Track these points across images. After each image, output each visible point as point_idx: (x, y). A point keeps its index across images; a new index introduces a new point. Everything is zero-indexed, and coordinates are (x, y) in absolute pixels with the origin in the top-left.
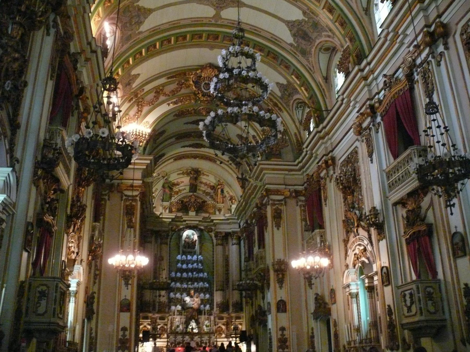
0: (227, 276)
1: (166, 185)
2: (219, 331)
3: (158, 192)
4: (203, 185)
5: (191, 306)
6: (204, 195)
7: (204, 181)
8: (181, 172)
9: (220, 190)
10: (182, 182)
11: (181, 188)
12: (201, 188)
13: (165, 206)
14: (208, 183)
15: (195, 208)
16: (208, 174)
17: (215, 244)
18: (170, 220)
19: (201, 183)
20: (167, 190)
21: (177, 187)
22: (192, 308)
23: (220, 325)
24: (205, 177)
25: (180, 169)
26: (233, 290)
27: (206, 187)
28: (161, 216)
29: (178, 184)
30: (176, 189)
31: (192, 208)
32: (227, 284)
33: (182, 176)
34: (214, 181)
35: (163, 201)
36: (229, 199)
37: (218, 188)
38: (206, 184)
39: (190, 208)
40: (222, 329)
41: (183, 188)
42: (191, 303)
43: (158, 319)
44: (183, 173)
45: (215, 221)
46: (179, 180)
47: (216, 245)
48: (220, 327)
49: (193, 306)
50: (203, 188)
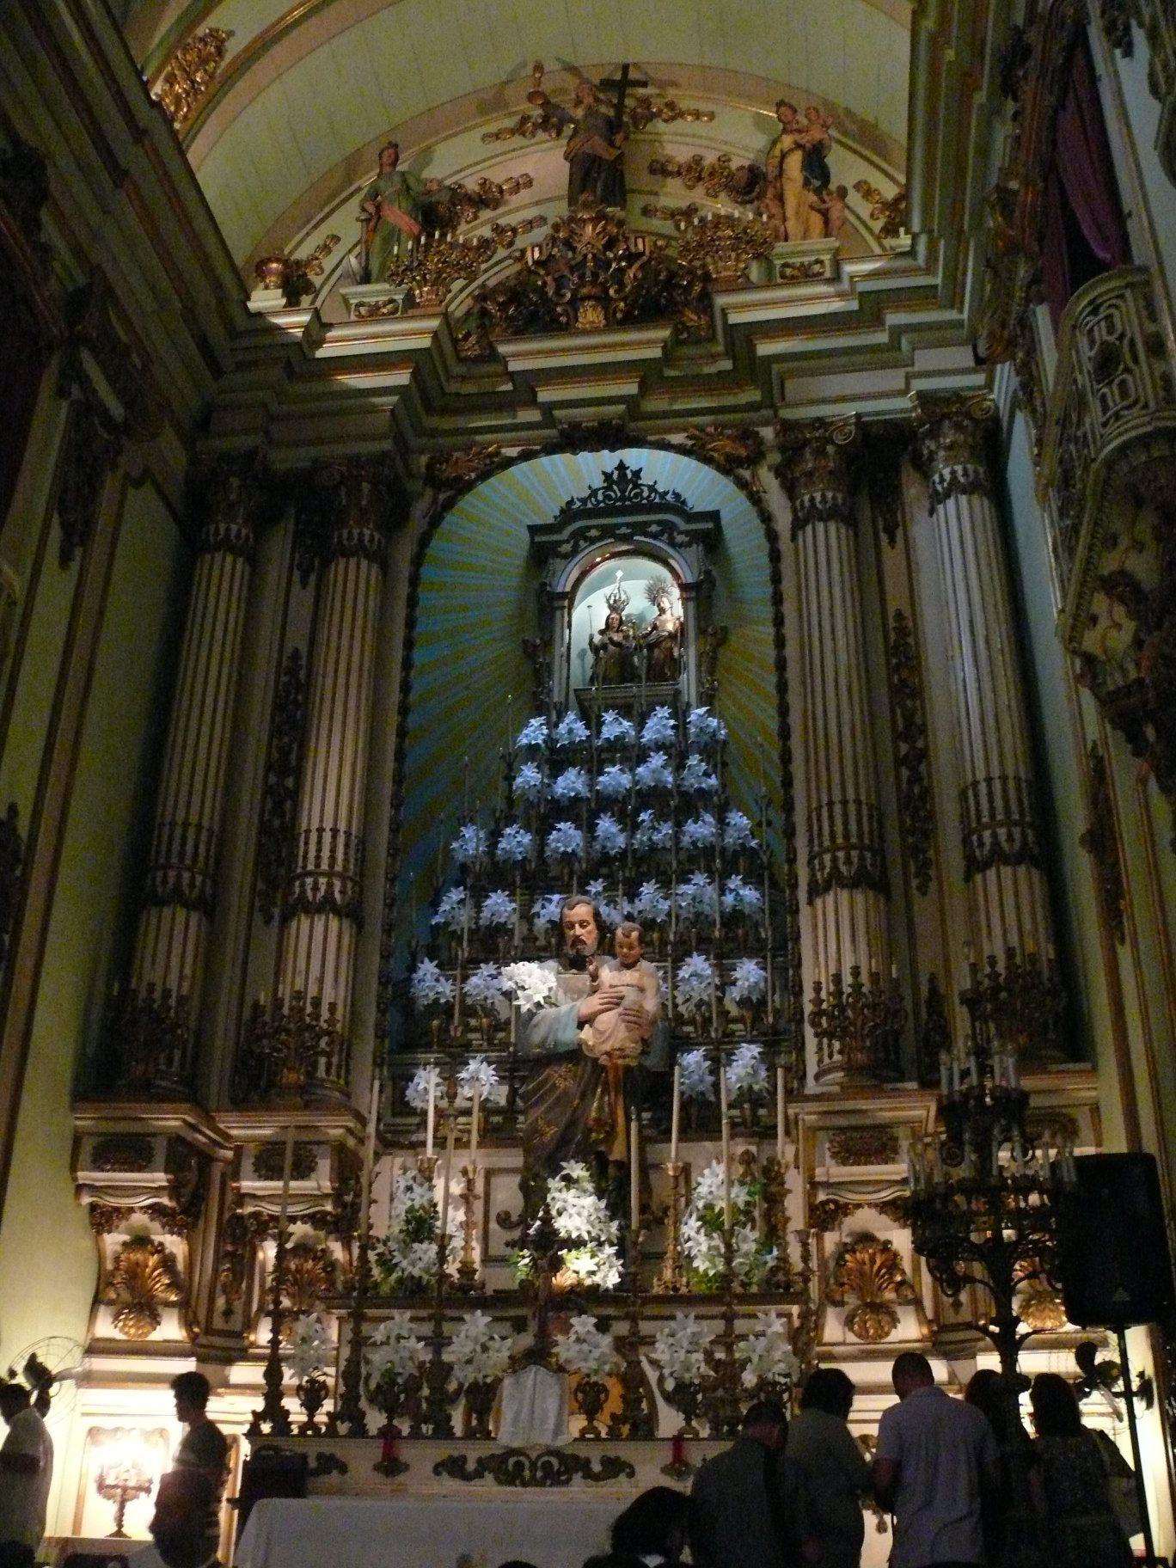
0: (916, 778)
2: (864, 1284)
3: (338, 251)
4: (674, 185)
5: (569, 1035)
8: (510, 123)
9: (795, 162)
15: (603, 300)
16: (703, 107)
17: (783, 521)
18: (402, 378)
19: (661, 169)
20: (398, 216)
21: (486, 214)
22: (575, 1055)
23: (866, 1219)
24: (686, 125)
25: (492, 103)
26: (974, 866)
27: (700, 190)
29: (487, 198)
30: (474, 229)
31: (590, 315)
32: (915, 851)
34: (759, 141)
36: (877, 226)
37: (784, 156)
38: (694, 172)
39: (575, 302)
42: (569, 1008)
43: (247, 1165)
44: (519, 129)
45: (765, 348)
46: (498, 176)
47: (798, 525)
48: (866, 1238)
49: (587, 1034)
50: (674, 195)
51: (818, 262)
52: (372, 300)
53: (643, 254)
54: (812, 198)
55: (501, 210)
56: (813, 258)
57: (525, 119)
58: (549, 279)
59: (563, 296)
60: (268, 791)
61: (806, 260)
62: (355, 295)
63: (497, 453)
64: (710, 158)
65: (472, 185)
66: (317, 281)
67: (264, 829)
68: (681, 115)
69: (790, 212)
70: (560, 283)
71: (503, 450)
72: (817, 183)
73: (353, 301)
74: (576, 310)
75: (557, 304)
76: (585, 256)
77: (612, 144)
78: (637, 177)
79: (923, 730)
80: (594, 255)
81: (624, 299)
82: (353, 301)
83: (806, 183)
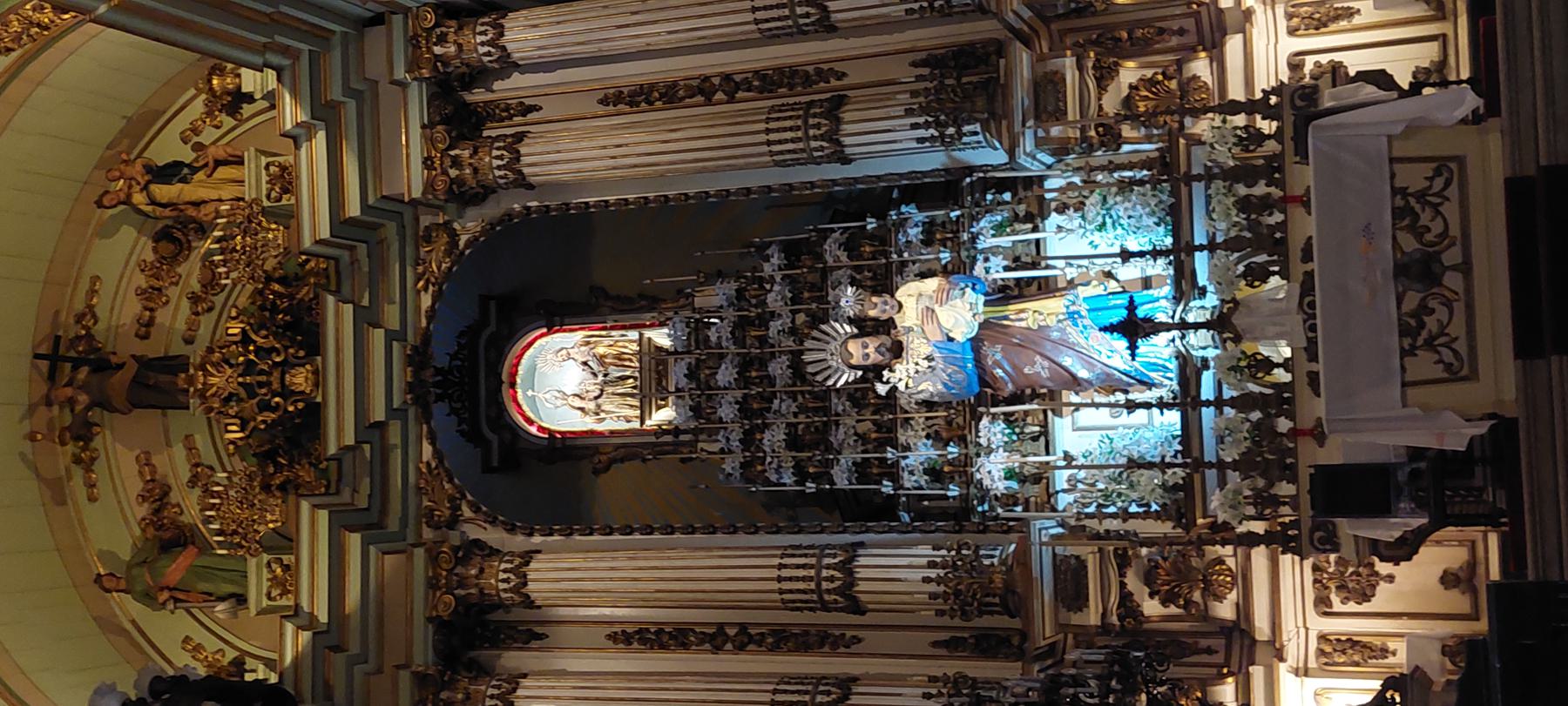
1: (145, 578)
3: (200, 635)
4: (162, 317)
6: (219, 300)
7: (132, 308)
9: (163, 192)
10: (145, 461)
11: (185, 474)
12: (181, 325)
13: (274, 580)
14: (141, 281)
15: (285, 366)
16: (84, 286)
18: (354, 541)
19: (146, 328)
21: (174, 497)
24: (102, 305)
27: (173, 292)
28: (323, 617)
29: (157, 494)
31: (300, 379)
32: (807, 80)
33: (100, 471)
34: (128, 234)
35: (241, 600)
37: (153, 202)
38: (152, 296)
39: (287, 393)
40: (1150, 83)
41: (179, 451)
44: (87, 465)
45: (353, 209)
46: (136, 486)
50: (175, 315)
51: (267, 167)
52: (266, 585)
53: (243, 329)
54: (201, 175)
55: (172, 481)
56: (264, 172)
57: (77, 460)
58: (260, 418)
59: (277, 403)
60: (740, 648)
61: (265, 178)
62: (259, 601)
63: (428, 464)
64: (141, 281)
65: (143, 510)
66: (231, 654)
67: (774, 649)
68: (91, 307)
69: (214, 195)
70: (265, 407)
71: (425, 459)
72: (186, 171)
73: (265, 602)
74: (293, 393)
75: (286, 410)
76: (240, 384)
77: (120, 366)
78: (153, 349)
79: (707, 79)
80: (240, 375)
81: (286, 348)
82: (265, 602)
83: (184, 180)
